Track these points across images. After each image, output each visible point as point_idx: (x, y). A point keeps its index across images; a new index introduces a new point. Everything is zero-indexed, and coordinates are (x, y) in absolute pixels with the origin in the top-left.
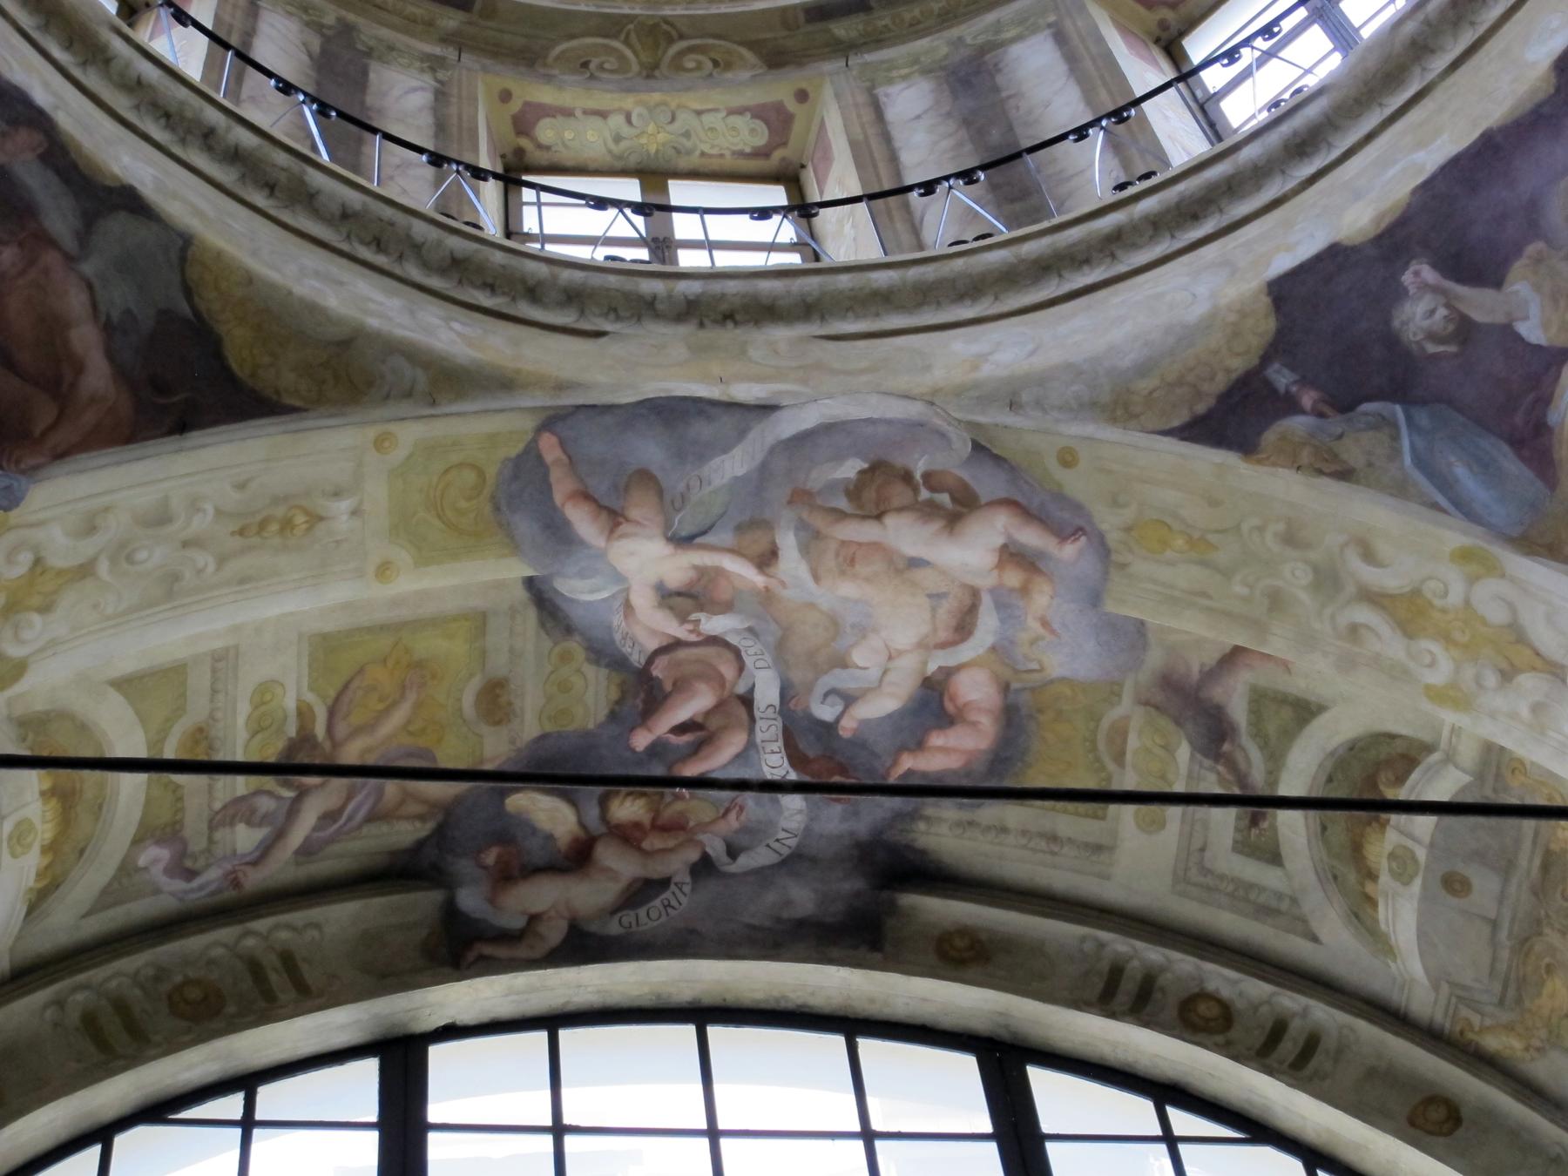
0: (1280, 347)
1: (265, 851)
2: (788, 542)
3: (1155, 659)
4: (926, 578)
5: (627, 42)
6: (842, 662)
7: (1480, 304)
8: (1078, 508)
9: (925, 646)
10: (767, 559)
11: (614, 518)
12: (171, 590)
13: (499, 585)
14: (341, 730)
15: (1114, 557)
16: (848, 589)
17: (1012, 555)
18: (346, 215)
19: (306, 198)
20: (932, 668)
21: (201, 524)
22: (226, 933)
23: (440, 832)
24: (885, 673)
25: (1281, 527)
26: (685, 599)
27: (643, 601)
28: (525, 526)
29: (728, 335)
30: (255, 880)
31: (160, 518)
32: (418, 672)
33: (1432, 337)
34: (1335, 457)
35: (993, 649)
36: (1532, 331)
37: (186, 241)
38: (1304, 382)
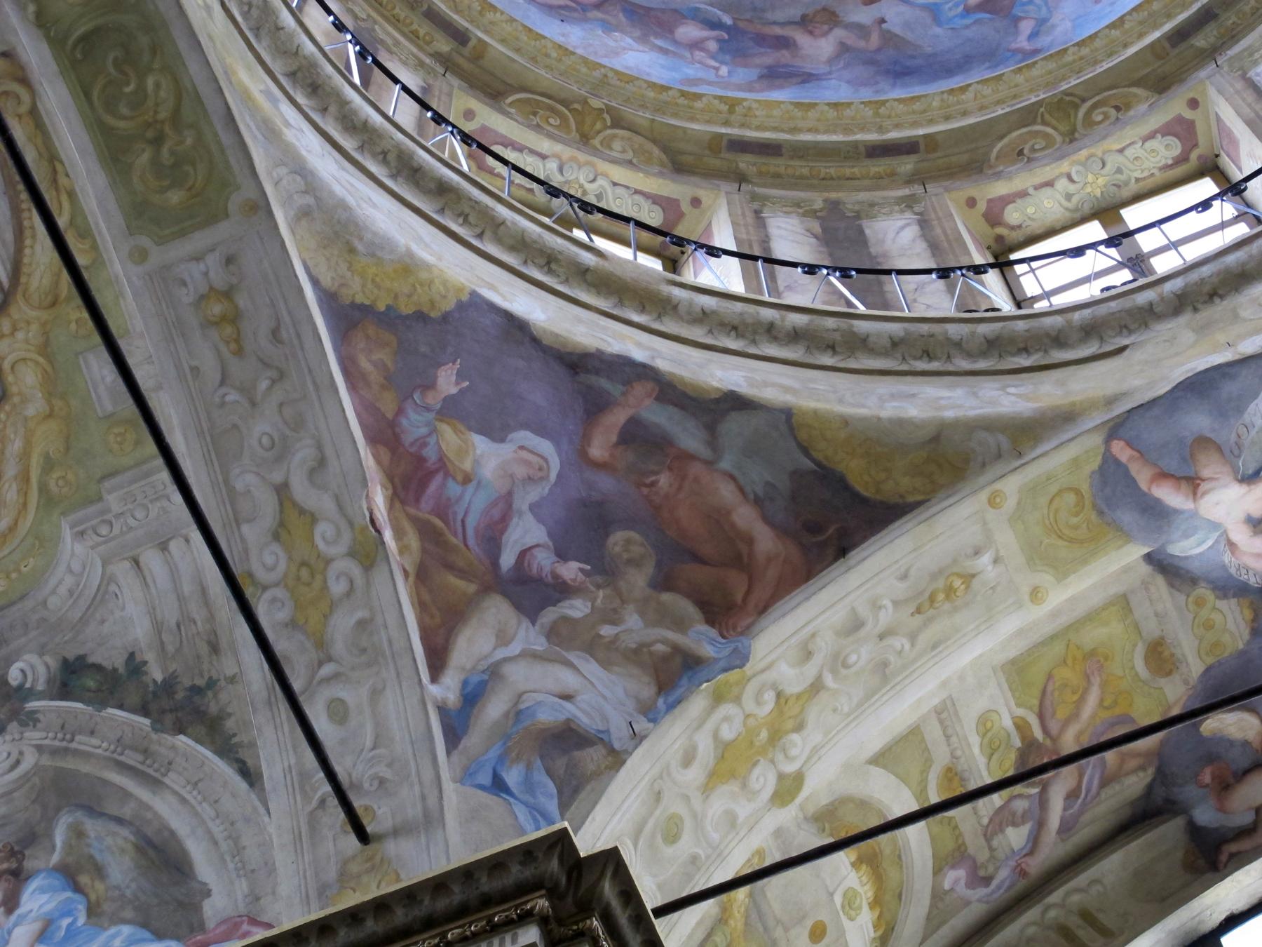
1: (1035, 840)
5: (1044, 123)
11: (1192, 483)
12: (884, 676)
13: (1127, 569)
14: (1054, 727)
19: (860, 344)
21: (886, 617)
22: (1032, 914)
23: (1162, 776)
27: (1241, 535)
28: (1127, 517)
29: (1220, 308)
30: (1036, 865)
31: (855, 625)
32: (1093, 660)
37: (788, 414)
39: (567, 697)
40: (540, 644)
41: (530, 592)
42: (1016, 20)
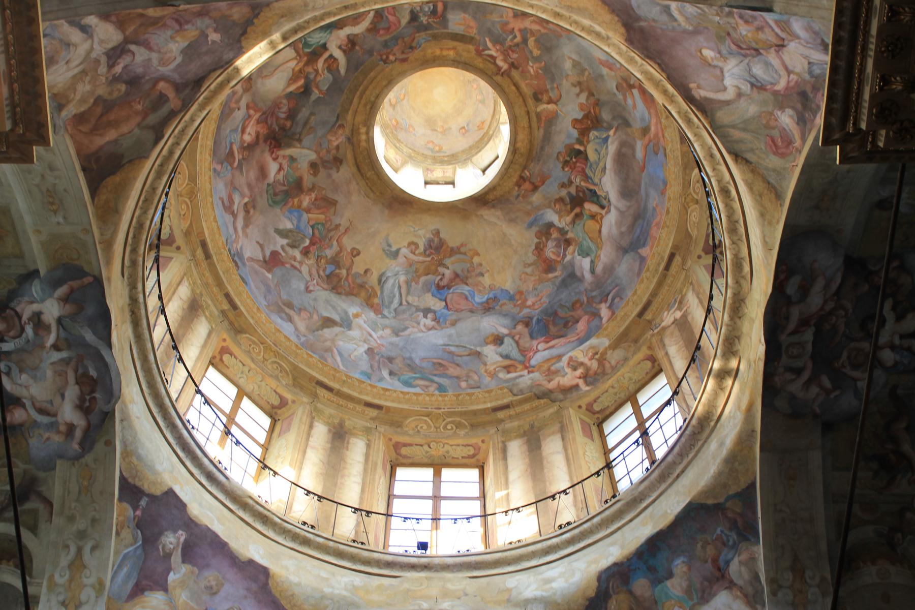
0: (152, 498)
2: (64, 355)
3: (41, 474)
4: (57, 400)
5: (188, 184)
6: (21, 371)
7: (177, 558)
8: (91, 448)
9: (32, 398)
10: (56, 347)
11: (65, 300)
13: (35, 262)
15: (76, 462)
16: (49, 373)
17: (71, 428)
18: (154, 189)
20: (24, 401)
24: (20, 385)
25: (97, 517)
26: (37, 319)
27: (35, 307)
31: (51, 168)
33: (164, 547)
34: (122, 528)
35: (35, 421)
36: (171, 577)
38: (144, 510)
39: (67, 63)
40: (94, 55)
41: (115, 54)
42: (222, 164)
